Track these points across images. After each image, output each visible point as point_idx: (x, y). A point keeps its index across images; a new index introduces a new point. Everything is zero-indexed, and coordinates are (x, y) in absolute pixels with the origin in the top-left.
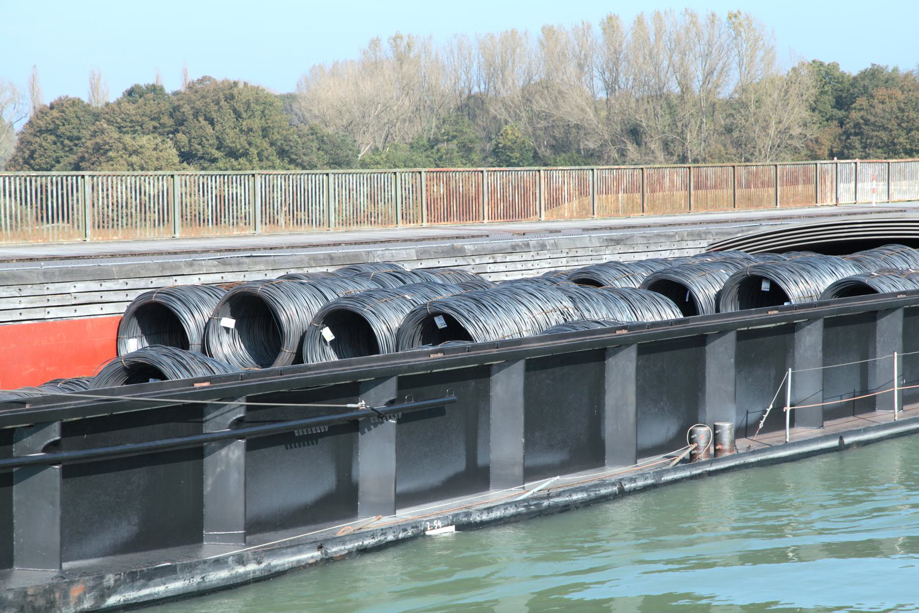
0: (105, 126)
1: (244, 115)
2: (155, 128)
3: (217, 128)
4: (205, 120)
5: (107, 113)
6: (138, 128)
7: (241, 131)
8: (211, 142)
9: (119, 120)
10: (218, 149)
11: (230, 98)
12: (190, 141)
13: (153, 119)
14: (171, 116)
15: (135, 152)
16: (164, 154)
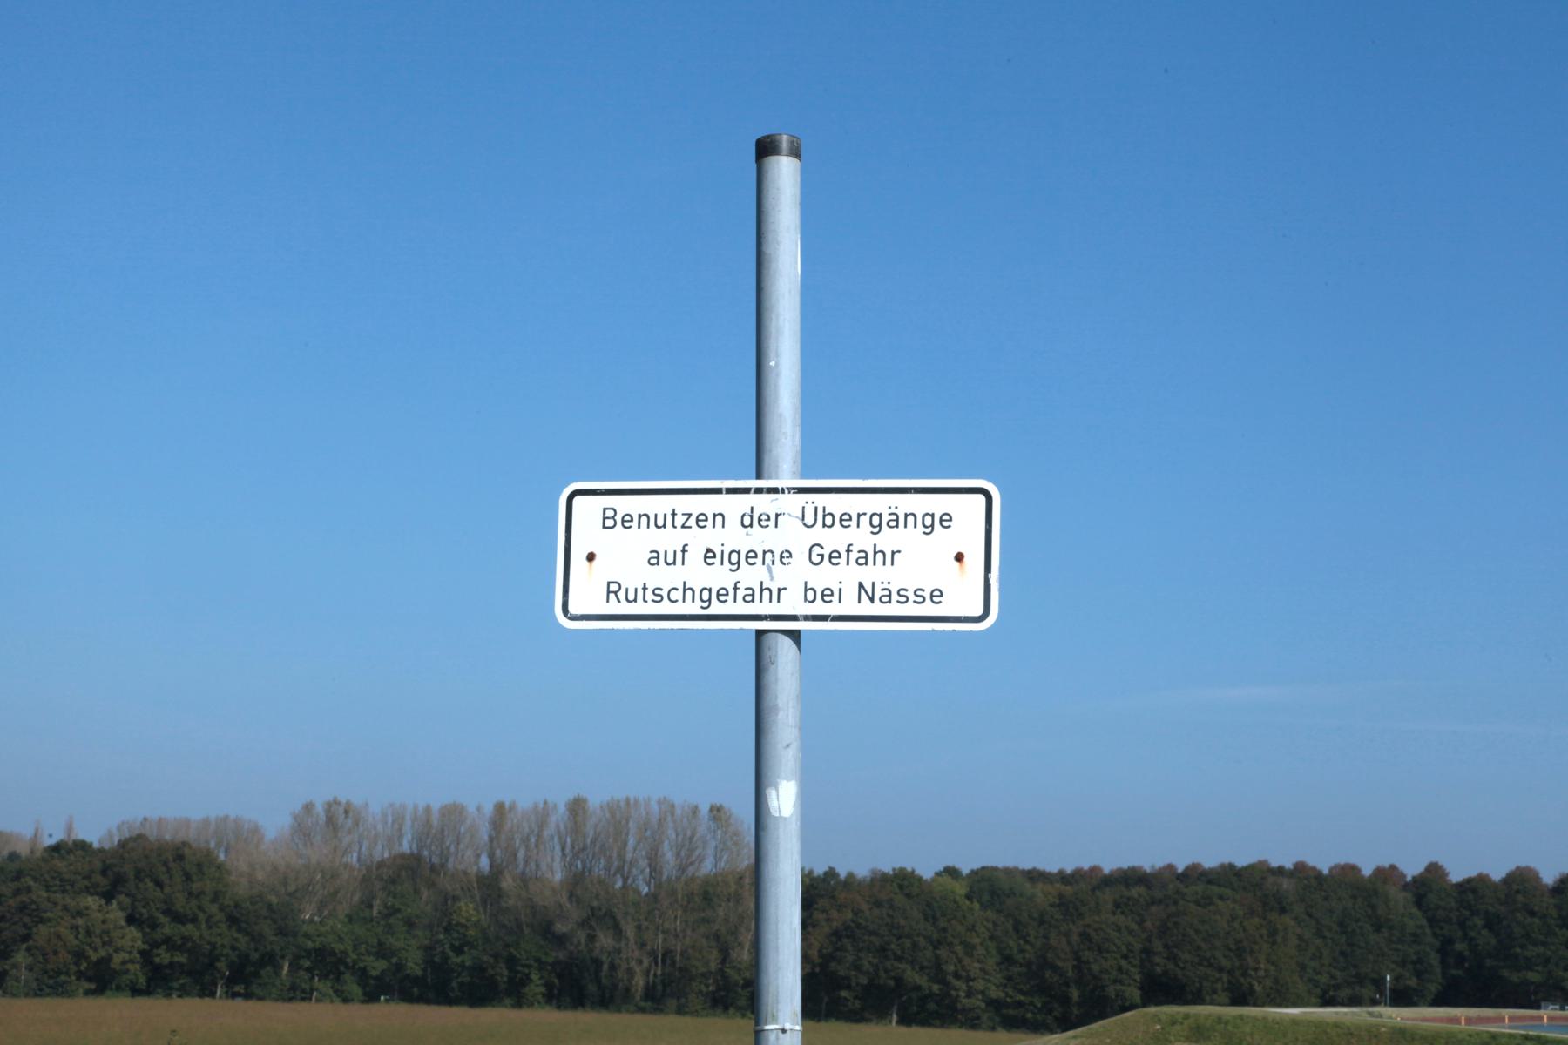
0: (32, 883)
1: (195, 878)
2: (87, 887)
3: (167, 890)
4: (151, 881)
5: (31, 870)
6: (68, 887)
7: (190, 894)
8: (158, 906)
9: (48, 878)
10: (164, 913)
11: (180, 857)
12: (132, 904)
13: (84, 878)
14: (104, 873)
15: (79, 913)
16: (111, 916)
